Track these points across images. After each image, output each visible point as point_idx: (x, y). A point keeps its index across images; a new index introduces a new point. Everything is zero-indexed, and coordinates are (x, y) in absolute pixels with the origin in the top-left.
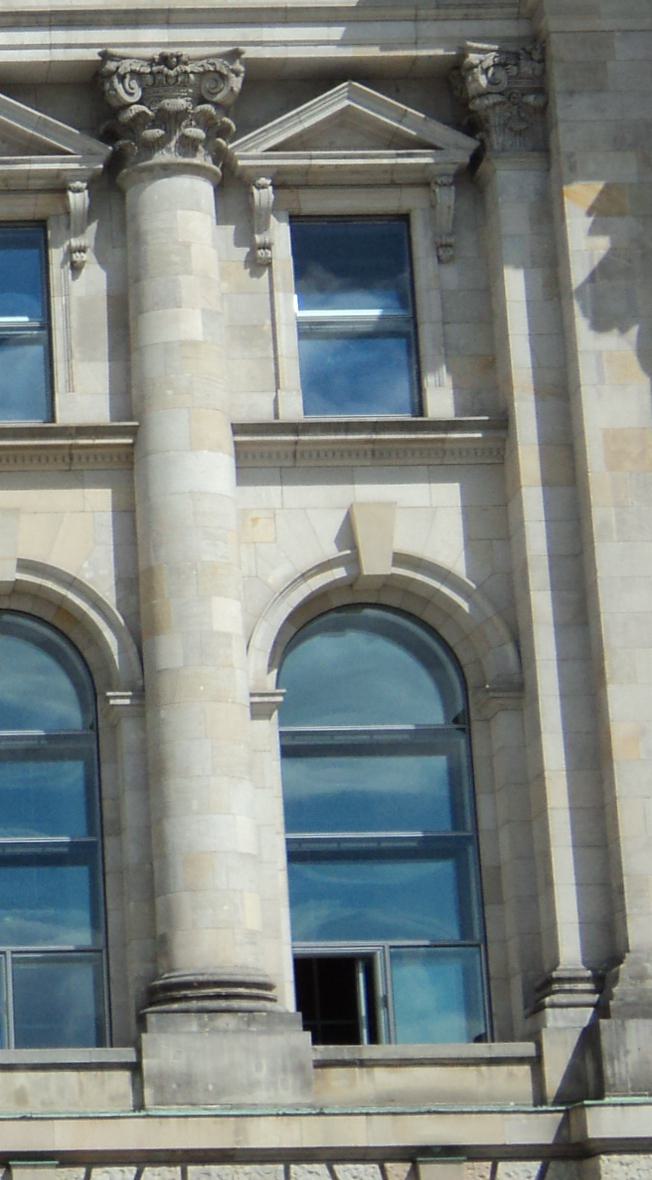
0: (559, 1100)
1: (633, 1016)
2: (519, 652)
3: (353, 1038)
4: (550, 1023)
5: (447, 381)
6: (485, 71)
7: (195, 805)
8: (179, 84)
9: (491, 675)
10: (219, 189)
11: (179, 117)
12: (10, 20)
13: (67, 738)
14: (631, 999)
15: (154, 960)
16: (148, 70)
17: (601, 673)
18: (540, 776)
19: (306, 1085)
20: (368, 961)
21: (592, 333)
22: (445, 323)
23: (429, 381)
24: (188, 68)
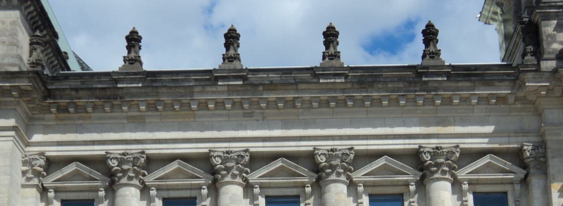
6: (529, 151)
8: (442, 155)
10: (453, 185)
11: (441, 164)
12: (393, 137)
16: (432, 151)
24: (444, 150)
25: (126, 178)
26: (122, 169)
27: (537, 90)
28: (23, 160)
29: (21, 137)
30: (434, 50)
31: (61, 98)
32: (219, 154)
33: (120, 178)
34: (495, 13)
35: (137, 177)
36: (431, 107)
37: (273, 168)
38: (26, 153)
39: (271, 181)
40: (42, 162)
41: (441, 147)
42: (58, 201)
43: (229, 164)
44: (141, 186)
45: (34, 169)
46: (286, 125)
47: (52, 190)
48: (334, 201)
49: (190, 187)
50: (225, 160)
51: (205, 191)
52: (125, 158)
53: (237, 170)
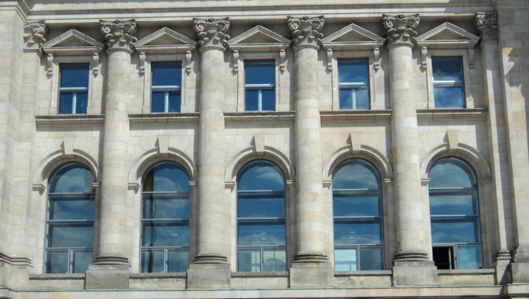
1: (520, 262)
3: (448, 268)
4: (499, 264)
5: (472, 99)
6: (482, 19)
7: (407, 208)
8: (403, 22)
9: (483, 175)
10: (413, 50)
11: (403, 31)
12: (359, 6)
13: (374, 191)
14: (519, 258)
16: (395, 19)
18: (496, 201)
19: (436, 280)
20: (452, 248)
21: (509, 87)
22: (471, 84)
23: (467, 99)
24: (405, 19)
25: (118, 44)
26: (114, 35)
28: (25, 27)
29: (23, 7)
32: (202, 22)
33: (112, 44)
35: (128, 43)
37: (251, 35)
38: (28, 21)
39: (249, 46)
40: (42, 29)
41: (403, 16)
43: (211, 31)
44: (131, 50)
45: (35, 36)
48: (306, 64)
49: (176, 52)
50: (207, 28)
51: (189, 56)
52: (117, 25)
53: (219, 37)
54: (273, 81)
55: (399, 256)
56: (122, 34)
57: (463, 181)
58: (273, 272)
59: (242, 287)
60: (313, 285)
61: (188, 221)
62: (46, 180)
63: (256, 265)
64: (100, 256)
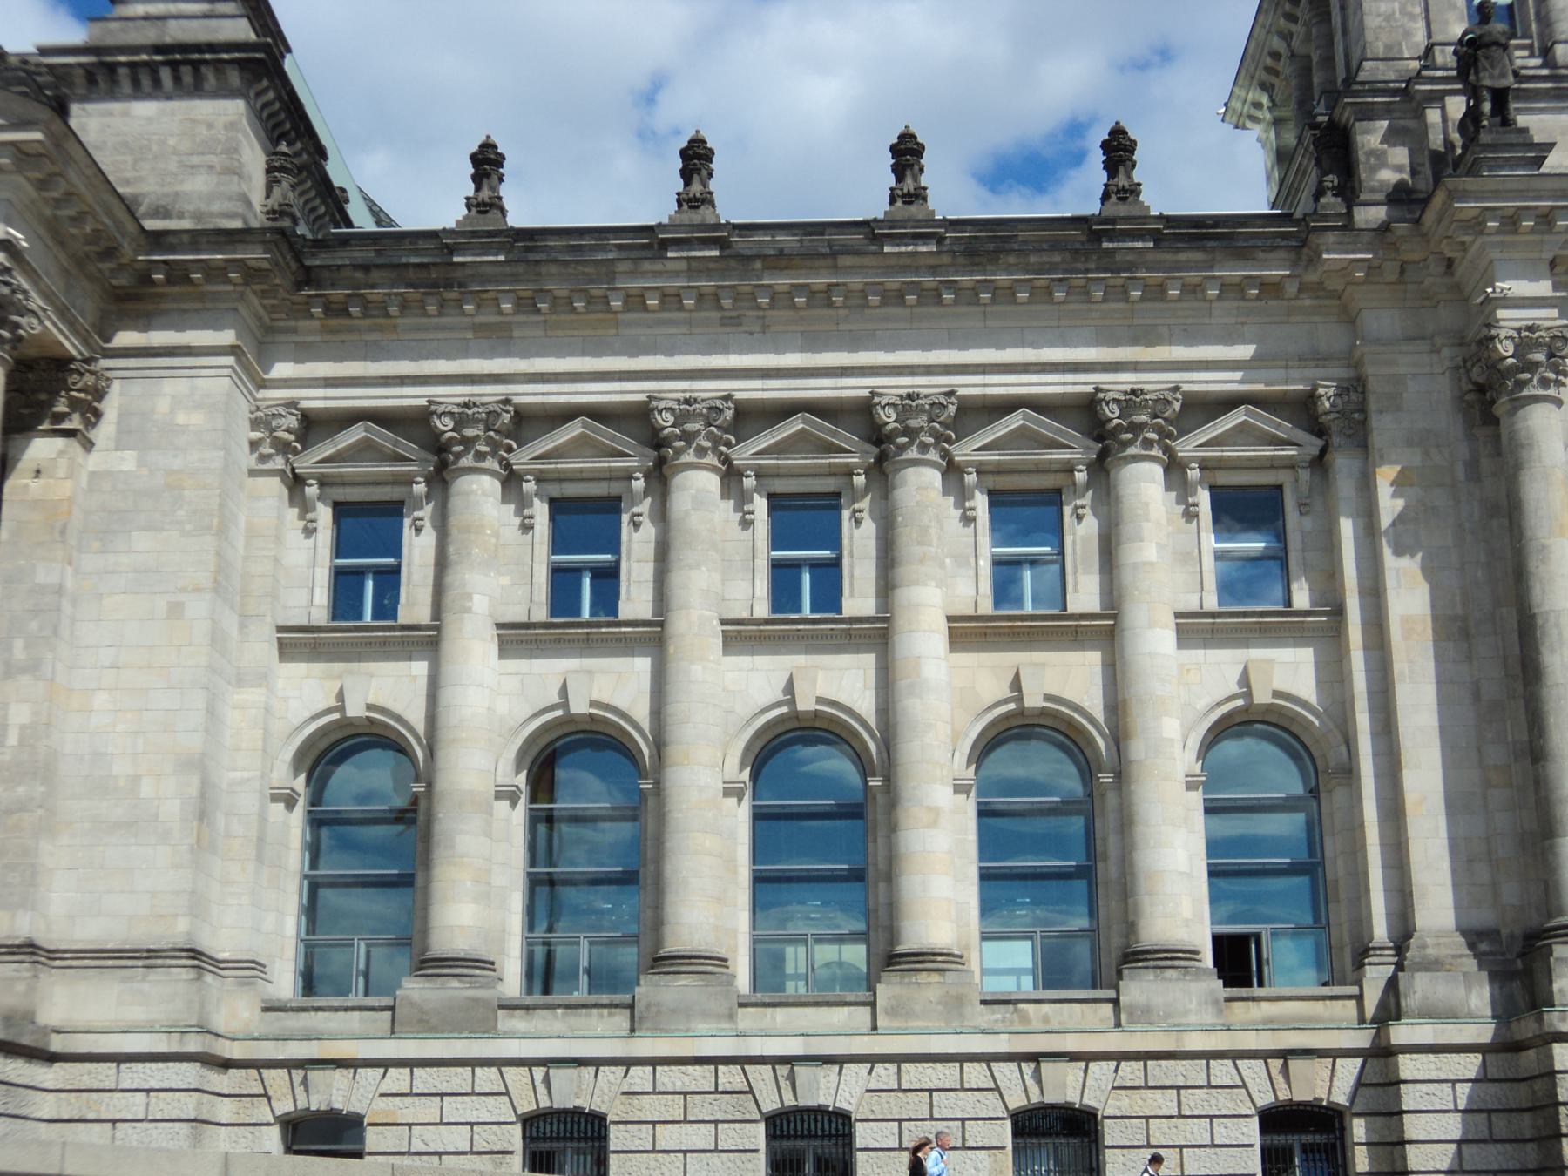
0: (1373, 1021)
1: (1418, 971)
2: (1349, 751)
3: (1250, 985)
4: (1368, 974)
5: (1306, 586)
6: (1329, 399)
7: (1152, 843)
8: (1143, 406)
9: (1332, 764)
10: (1167, 470)
11: (1142, 426)
13: (1074, 802)
14: (1417, 960)
15: (1127, 937)
17: (1399, 762)
18: (1362, 825)
19: (1220, 1012)
20: (1258, 937)
21: (1394, 557)
22: (1304, 551)
23: (1294, 586)
25: (470, 456)
26: (462, 436)
27: (1347, 268)
28: (253, 416)
29: (248, 369)
30: (1126, 184)
31: (333, 286)
33: (458, 456)
34: (1257, 105)
35: (494, 454)
36: (1121, 305)
37: (784, 435)
38: (259, 403)
40: (293, 422)
42: (325, 505)
43: (692, 427)
46: (813, 343)
47: (314, 482)
48: (914, 504)
51: (639, 484)
52: (470, 412)
54: (835, 542)
55: (1134, 957)
56: (481, 433)
57: (1285, 780)
58: (838, 993)
59: (762, 1030)
60: (930, 1024)
61: (637, 873)
62: (302, 777)
63: (796, 977)
64: (430, 955)
